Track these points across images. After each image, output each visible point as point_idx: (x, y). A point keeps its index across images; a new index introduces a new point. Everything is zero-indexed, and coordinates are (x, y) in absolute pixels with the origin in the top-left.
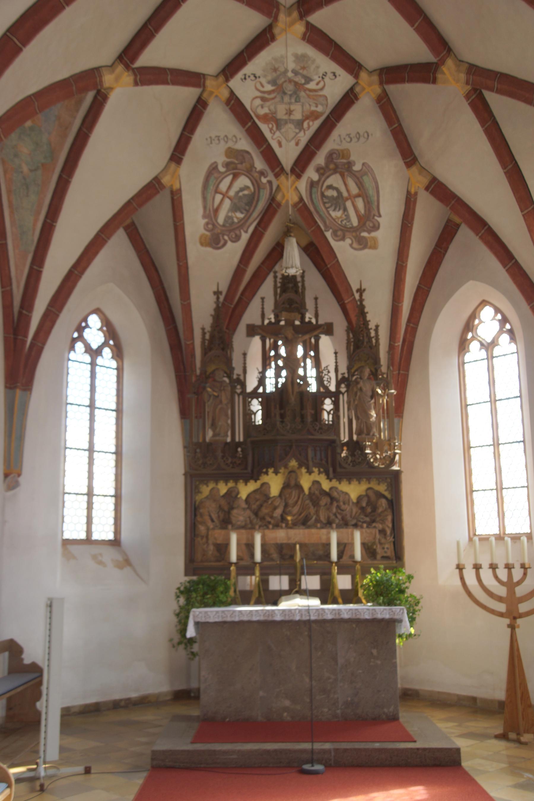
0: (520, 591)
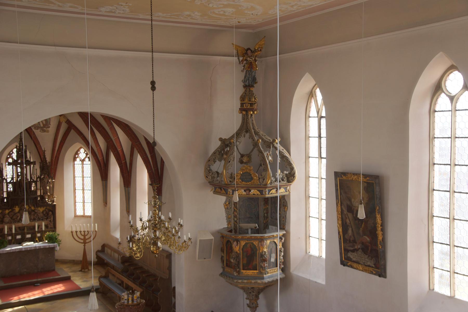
0: (87, 237)
